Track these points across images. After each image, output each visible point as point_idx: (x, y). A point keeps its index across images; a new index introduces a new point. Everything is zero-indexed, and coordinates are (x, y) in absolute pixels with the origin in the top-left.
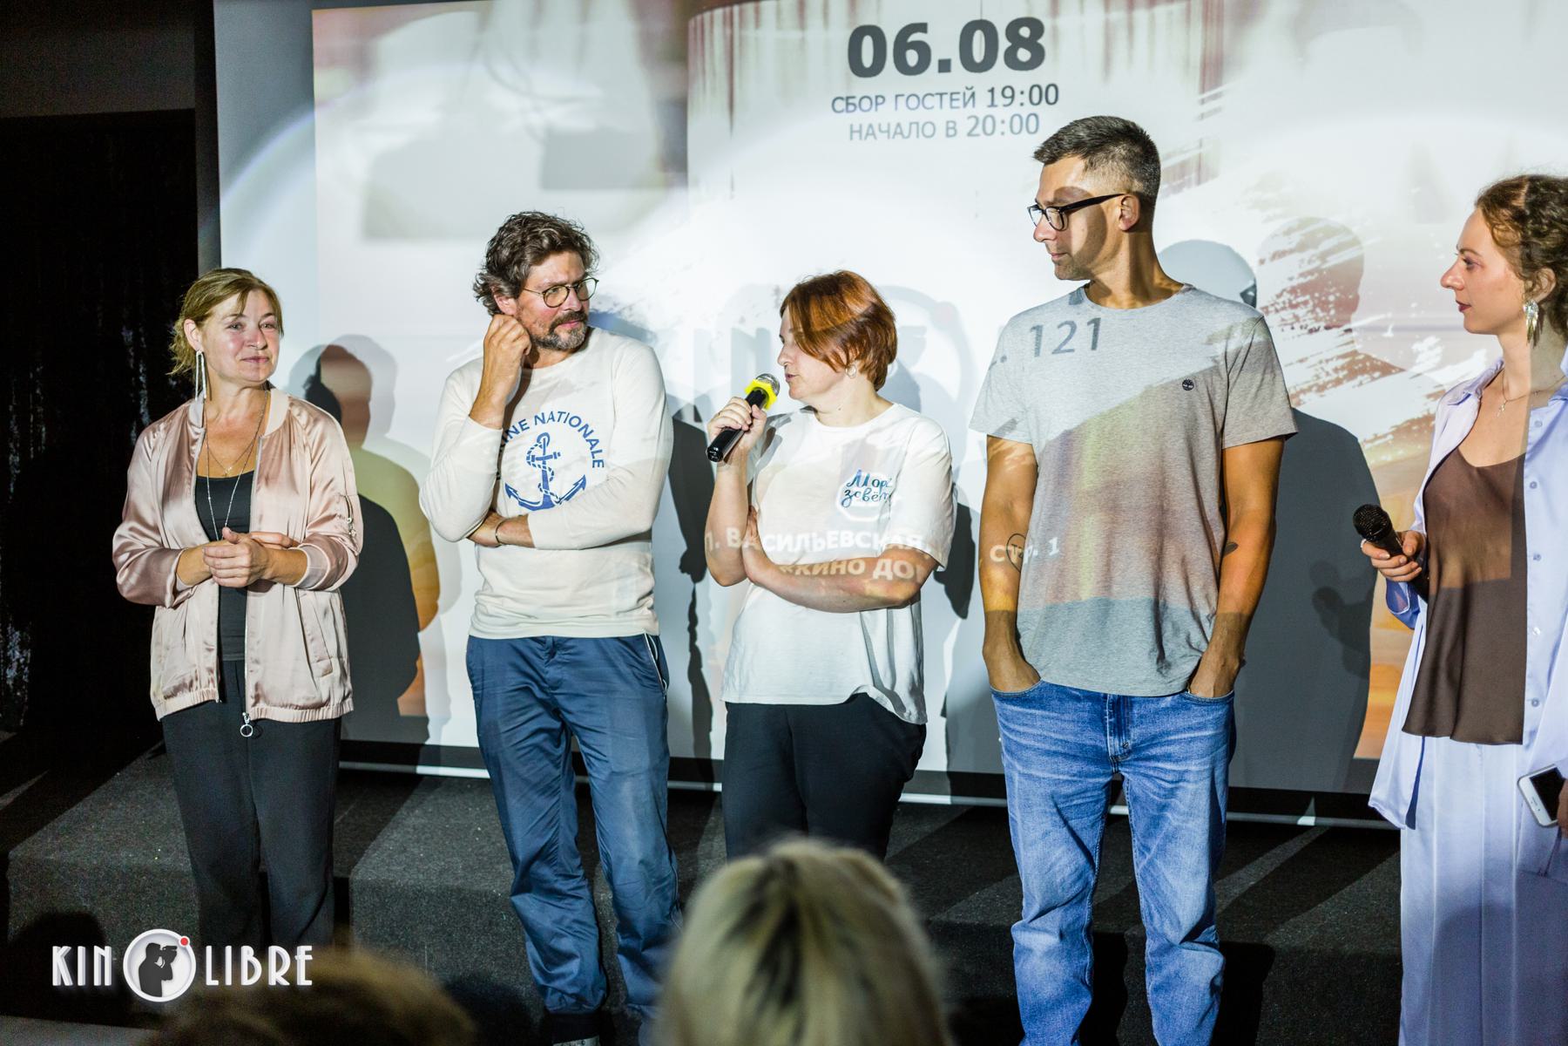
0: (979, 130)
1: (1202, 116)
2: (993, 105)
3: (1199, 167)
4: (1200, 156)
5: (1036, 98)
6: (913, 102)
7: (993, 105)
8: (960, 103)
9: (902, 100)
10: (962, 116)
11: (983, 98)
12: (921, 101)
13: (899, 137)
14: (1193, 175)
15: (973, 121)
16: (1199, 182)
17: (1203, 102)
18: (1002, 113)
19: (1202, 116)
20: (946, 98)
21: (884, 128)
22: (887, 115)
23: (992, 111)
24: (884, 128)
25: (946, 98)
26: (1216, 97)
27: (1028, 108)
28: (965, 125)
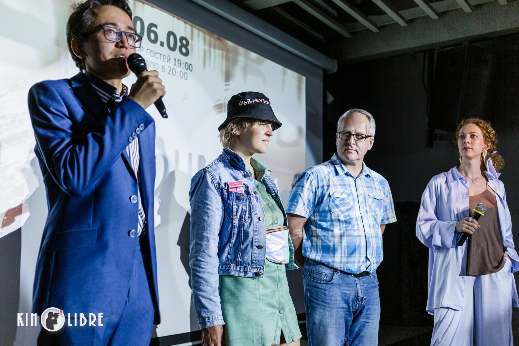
0: (171, 73)
1: (225, 90)
2: (175, 65)
7: (175, 65)
8: (166, 60)
9: (149, 51)
10: (166, 65)
11: (172, 61)
15: (169, 69)
17: (226, 85)
18: (178, 69)
19: (225, 90)
20: (162, 56)
23: (174, 67)
25: (162, 56)
26: (228, 85)
27: (184, 71)
28: (167, 70)
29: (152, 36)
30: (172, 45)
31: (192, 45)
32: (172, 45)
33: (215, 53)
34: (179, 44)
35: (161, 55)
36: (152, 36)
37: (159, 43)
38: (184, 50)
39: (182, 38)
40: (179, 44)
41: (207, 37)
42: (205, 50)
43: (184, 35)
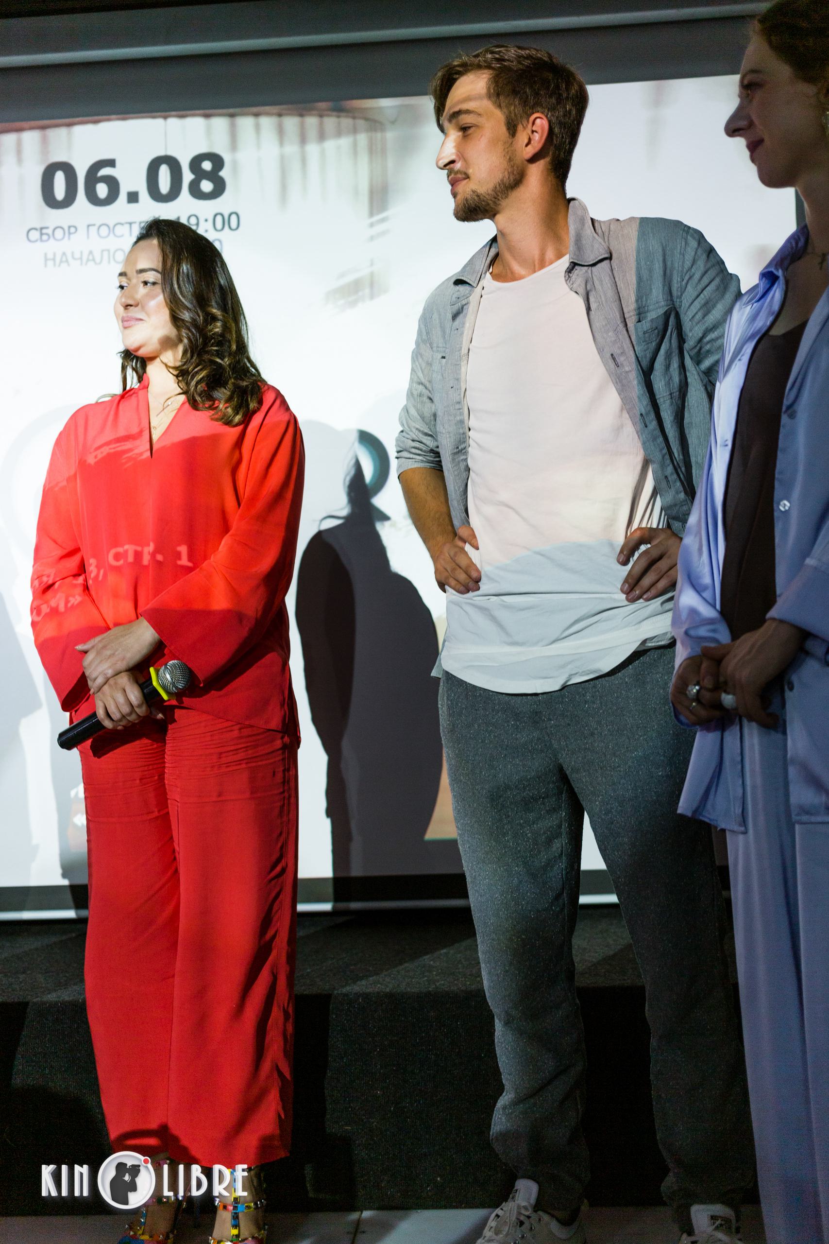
1: (372, 238)
3: (372, 285)
4: (372, 274)
5: (219, 225)
6: (104, 231)
9: (93, 230)
12: (112, 229)
13: (91, 263)
14: (367, 291)
16: (372, 297)
17: (372, 225)
19: (372, 238)
21: (77, 255)
22: (78, 243)
24: (77, 255)
26: (383, 220)
29: (102, 190)
30: (164, 185)
31: (235, 163)
32: (164, 185)
33: (323, 154)
34: (188, 176)
35: (130, 224)
36: (102, 190)
37: (123, 196)
38: (207, 186)
39: (196, 163)
40: (188, 176)
41: (291, 123)
42: (283, 159)
43: (204, 150)
